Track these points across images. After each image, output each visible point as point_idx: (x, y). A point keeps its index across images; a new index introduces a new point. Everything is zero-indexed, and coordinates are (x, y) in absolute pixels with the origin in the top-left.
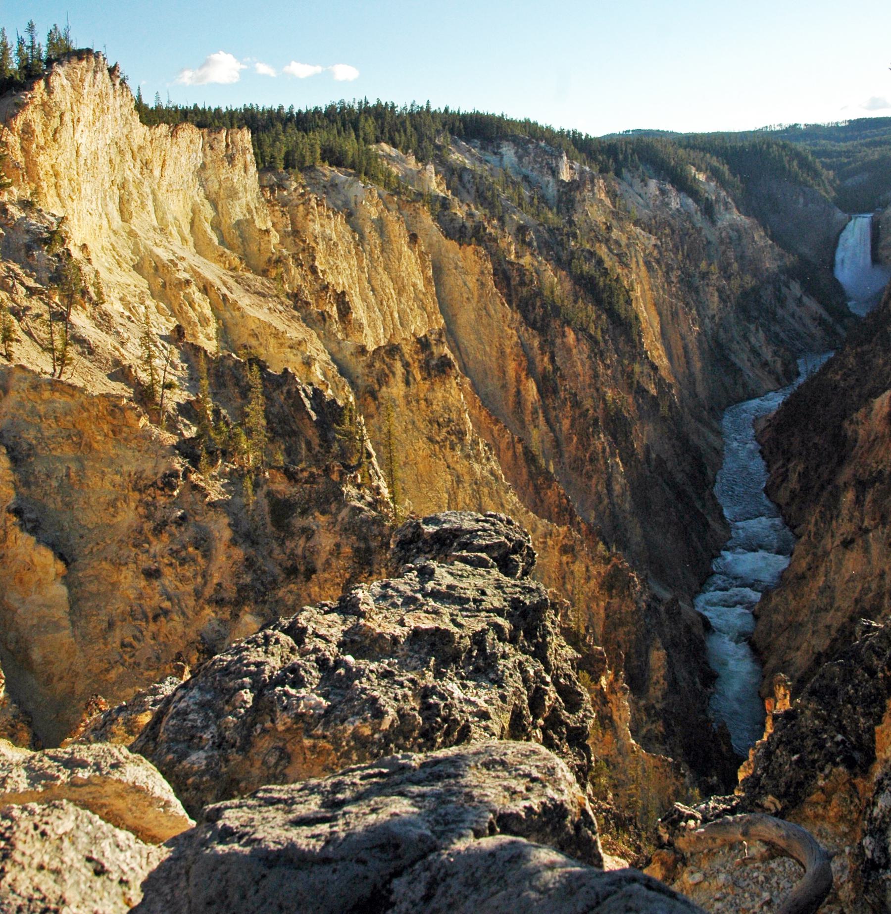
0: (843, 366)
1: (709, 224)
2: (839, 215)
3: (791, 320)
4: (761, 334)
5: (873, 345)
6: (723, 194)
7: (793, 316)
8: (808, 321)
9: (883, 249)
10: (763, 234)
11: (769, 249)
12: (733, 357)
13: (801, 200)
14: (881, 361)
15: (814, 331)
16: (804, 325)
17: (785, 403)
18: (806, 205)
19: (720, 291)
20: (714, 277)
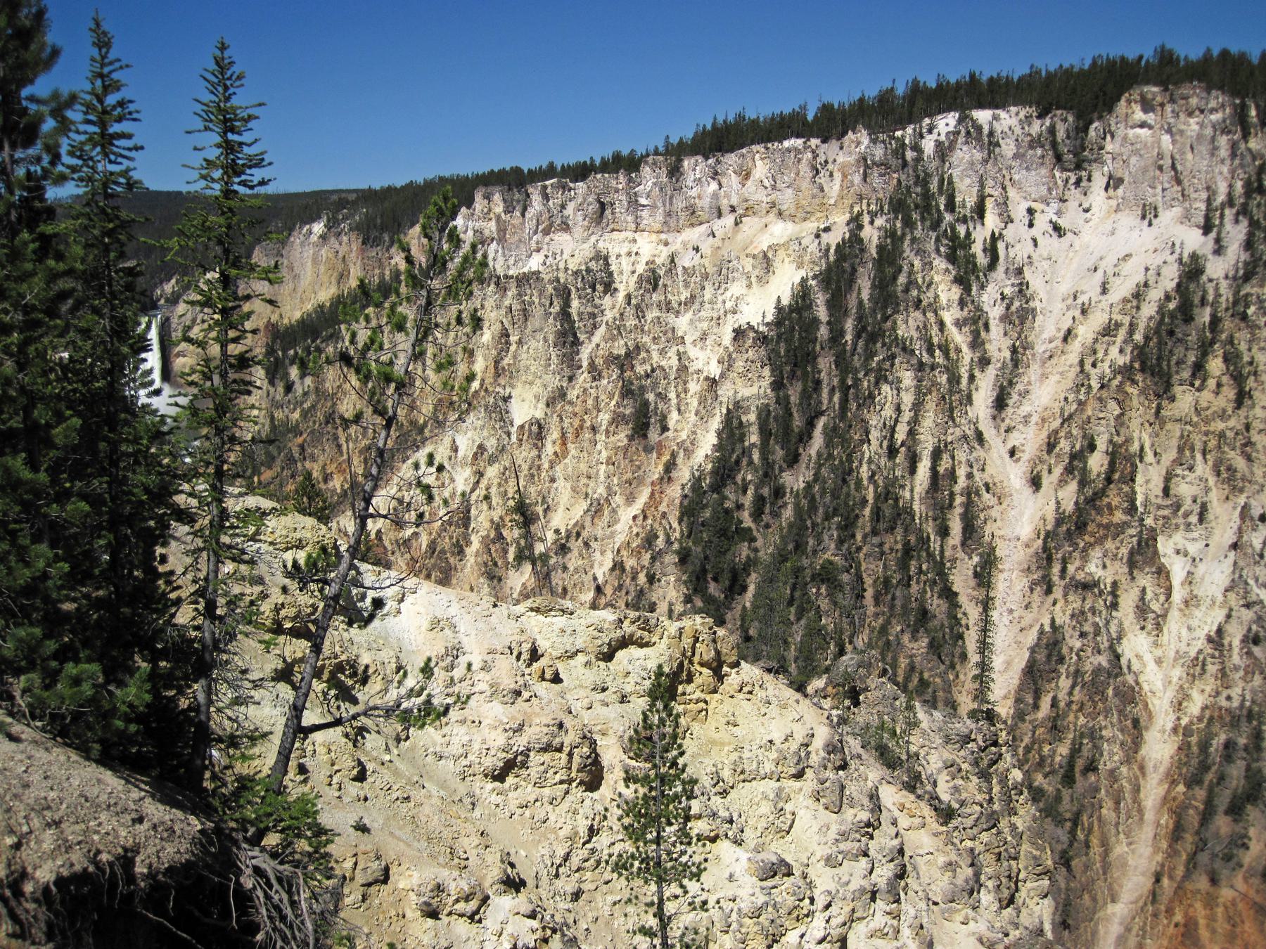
9: (178, 355)
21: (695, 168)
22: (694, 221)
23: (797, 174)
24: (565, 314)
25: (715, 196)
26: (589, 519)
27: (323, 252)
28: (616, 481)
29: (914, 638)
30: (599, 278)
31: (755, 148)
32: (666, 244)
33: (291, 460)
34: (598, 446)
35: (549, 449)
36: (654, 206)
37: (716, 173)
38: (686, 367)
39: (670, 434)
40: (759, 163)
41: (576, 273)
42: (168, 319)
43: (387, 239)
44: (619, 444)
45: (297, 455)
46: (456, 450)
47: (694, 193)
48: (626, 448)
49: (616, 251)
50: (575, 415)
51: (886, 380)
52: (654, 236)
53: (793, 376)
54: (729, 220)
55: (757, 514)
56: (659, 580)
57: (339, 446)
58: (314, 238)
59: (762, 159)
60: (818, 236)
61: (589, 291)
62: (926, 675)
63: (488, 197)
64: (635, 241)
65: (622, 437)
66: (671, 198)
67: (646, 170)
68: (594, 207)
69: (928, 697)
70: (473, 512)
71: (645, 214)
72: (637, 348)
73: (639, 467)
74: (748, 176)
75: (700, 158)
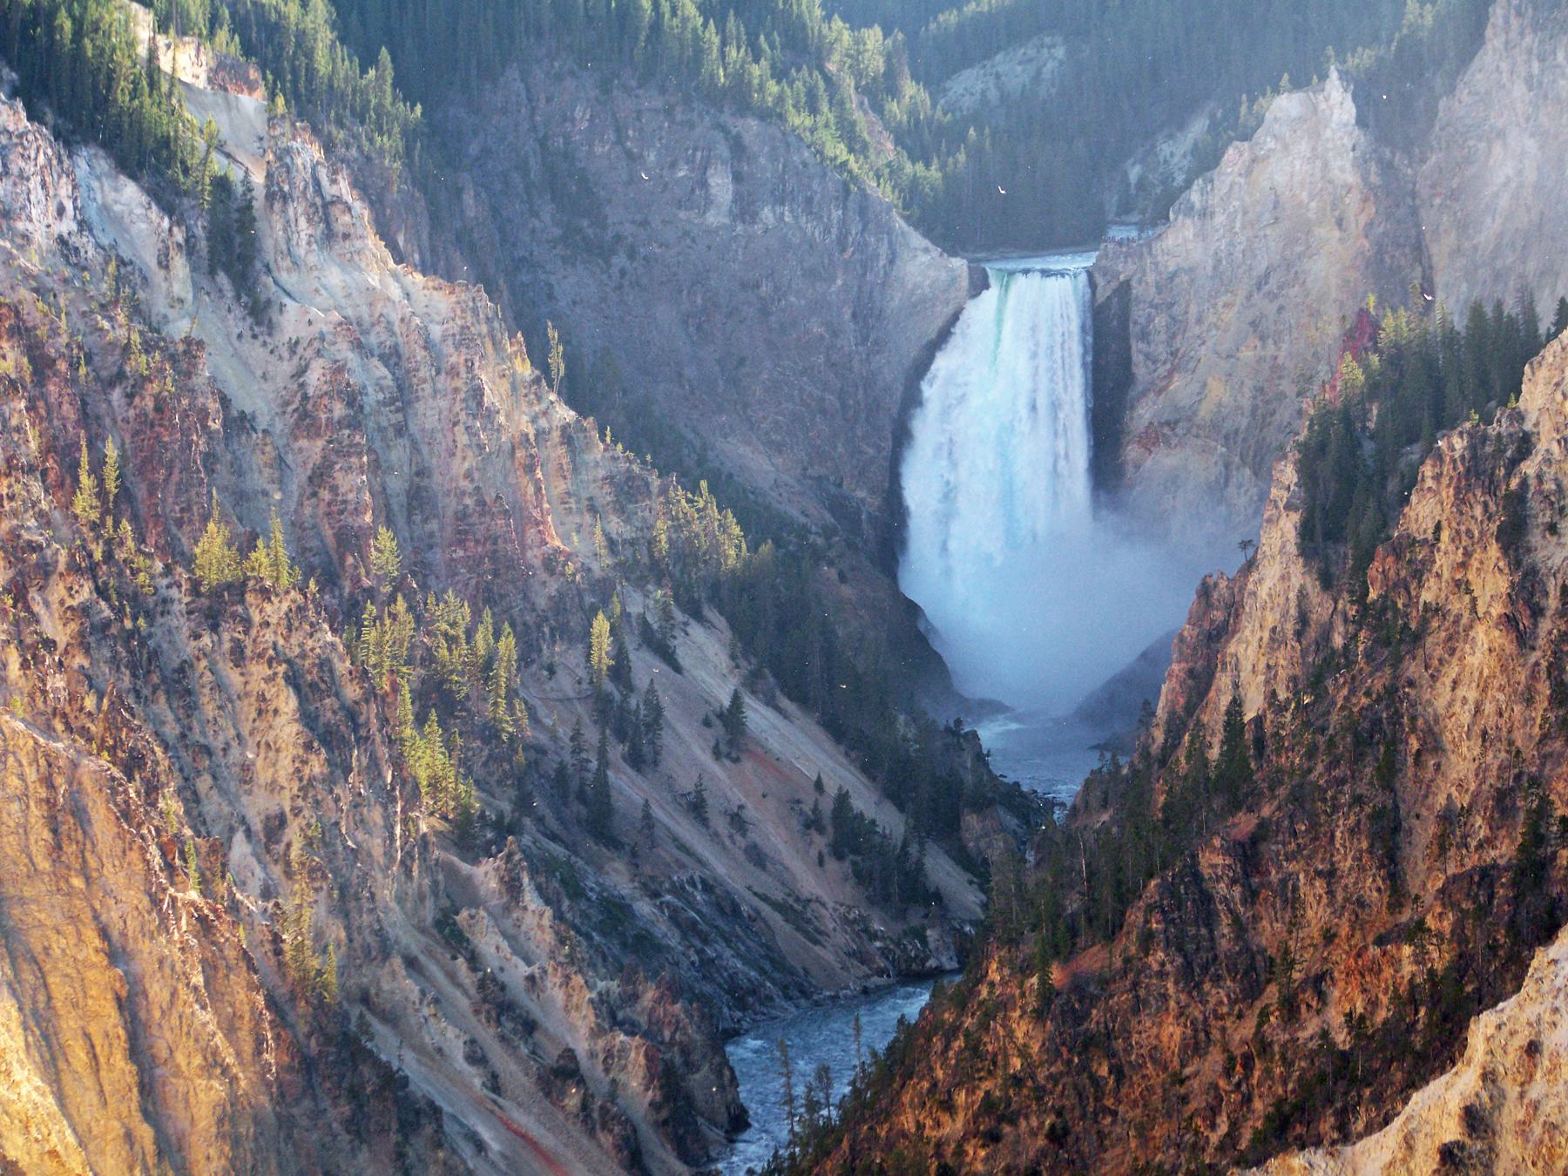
0: (976, 1060)
1: (237, 322)
2: (923, 265)
3: (686, 830)
4: (535, 914)
5: (1129, 943)
6: (309, 153)
7: (697, 808)
9: (1153, 438)
10: (525, 370)
11: (557, 453)
12: (386, 1045)
13: (721, 185)
15: (809, 883)
16: (757, 857)
18: (744, 209)
19: (309, 685)
20: (276, 610)
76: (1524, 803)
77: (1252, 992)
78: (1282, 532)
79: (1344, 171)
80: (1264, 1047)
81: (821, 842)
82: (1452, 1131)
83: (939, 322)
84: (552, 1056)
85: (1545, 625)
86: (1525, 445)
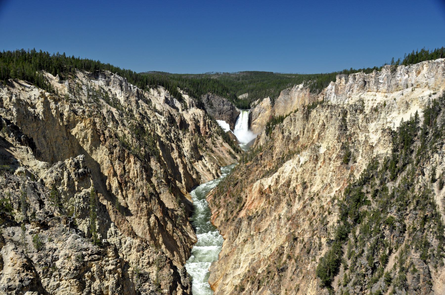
2: (237, 110)
5: (252, 162)
6: (191, 100)
8: (225, 152)
9: (254, 124)
12: (195, 167)
13: (222, 104)
14: (255, 168)
17: (217, 186)
21: (401, 69)
22: (398, 89)
23: (437, 72)
24: (344, 120)
25: (406, 80)
26: (322, 190)
27: (301, 94)
28: (334, 178)
29: (416, 252)
30: (359, 108)
31: (424, 62)
32: (386, 97)
33: (257, 160)
34: (331, 165)
35: (319, 164)
36: (384, 83)
37: (408, 72)
38: (368, 141)
39: (357, 164)
40: (425, 68)
41: (351, 106)
42: (252, 112)
43: (318, 91)
44: (338, 165)
45: (259, 158)
46: (299, 162)
47: (398, 79)
48: (339, 167)
49: (368, 99)
50: (330, 154)
51: (437, 152)
52: (383, 94)
53: (402, 147)
54: (410, 89)
55: (374, 196)
56: (332, 214)
57: (272, 157)
58: (299, 89)
59: (427, 66)
60: (430, 96)
61: (354, 112)
62: (416, 267)
63: (340, 78)
64: (376, 95)
65: (339, 163)
66: (391, 80)
67: (384, 70)
68: (362, 82)
69: (415, 276)
70: (292, 182)
71: (381, 86)
72: (354, 133)
73: (343, 174)
74: (419, 72)
75: (403, 66)
76: (282, 153)
77: (261, 166)
78: (264, 132)
79: (269, 105)
80: (262, 170)
81: (228, 153)
82: (277, 177)
83: (237, 115)
84: (207, 168)
85: (285, 140)
86: (283, 126)
